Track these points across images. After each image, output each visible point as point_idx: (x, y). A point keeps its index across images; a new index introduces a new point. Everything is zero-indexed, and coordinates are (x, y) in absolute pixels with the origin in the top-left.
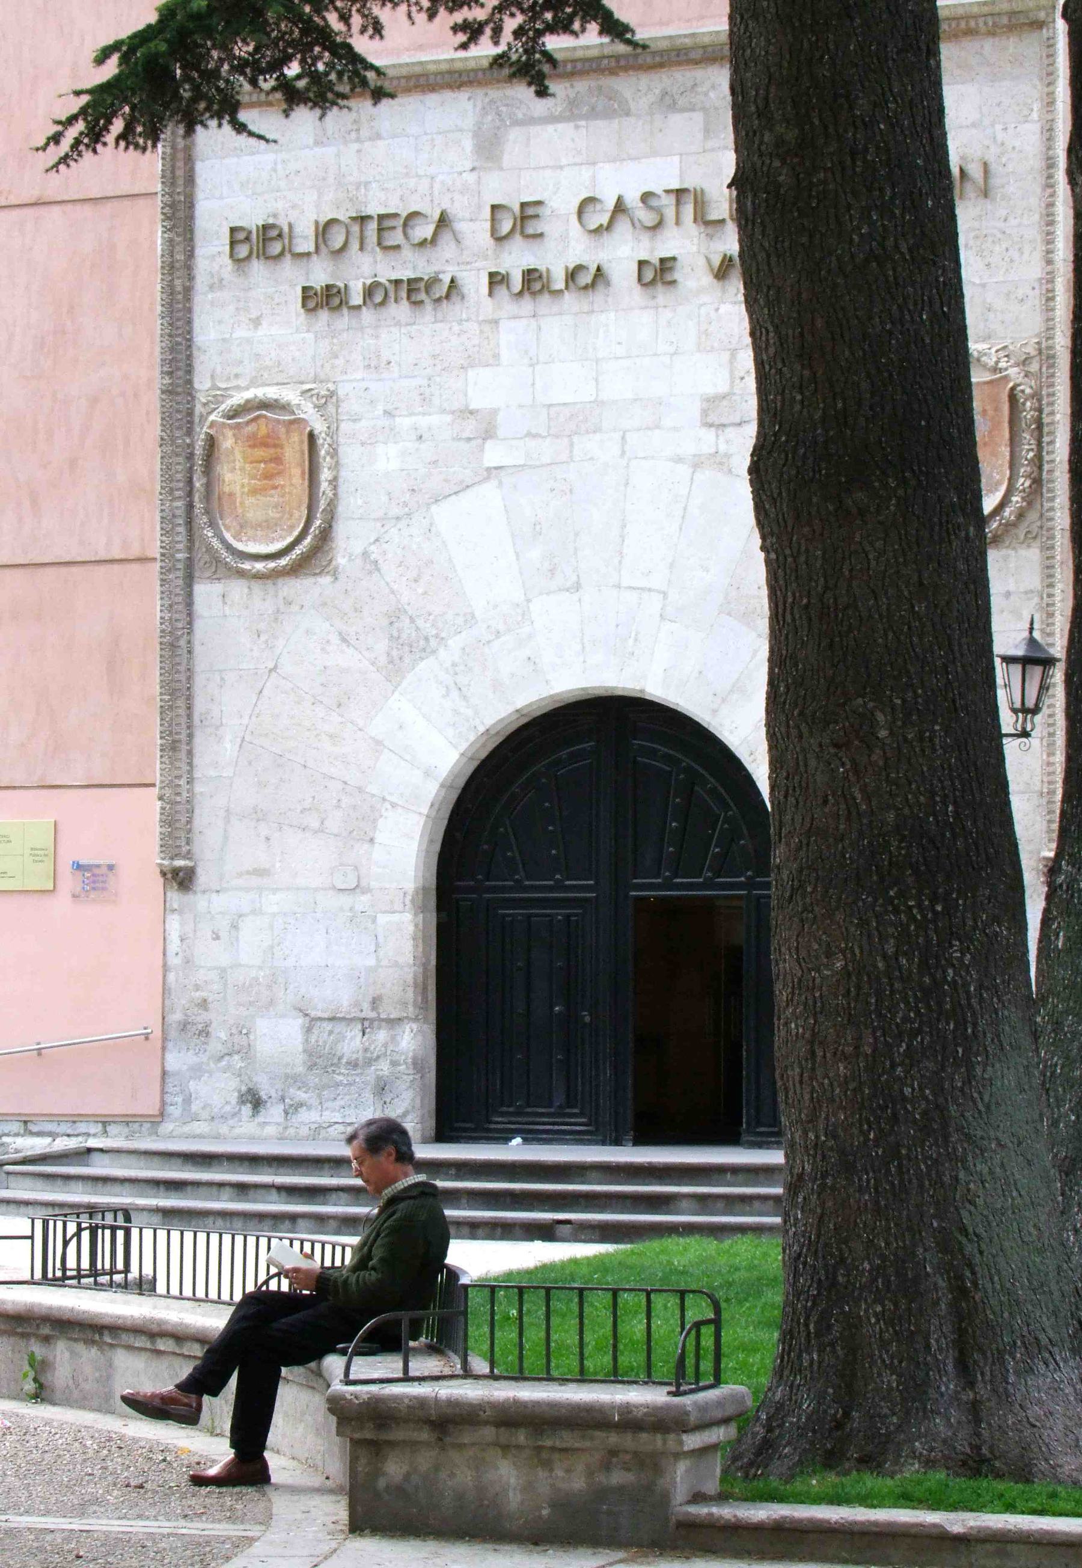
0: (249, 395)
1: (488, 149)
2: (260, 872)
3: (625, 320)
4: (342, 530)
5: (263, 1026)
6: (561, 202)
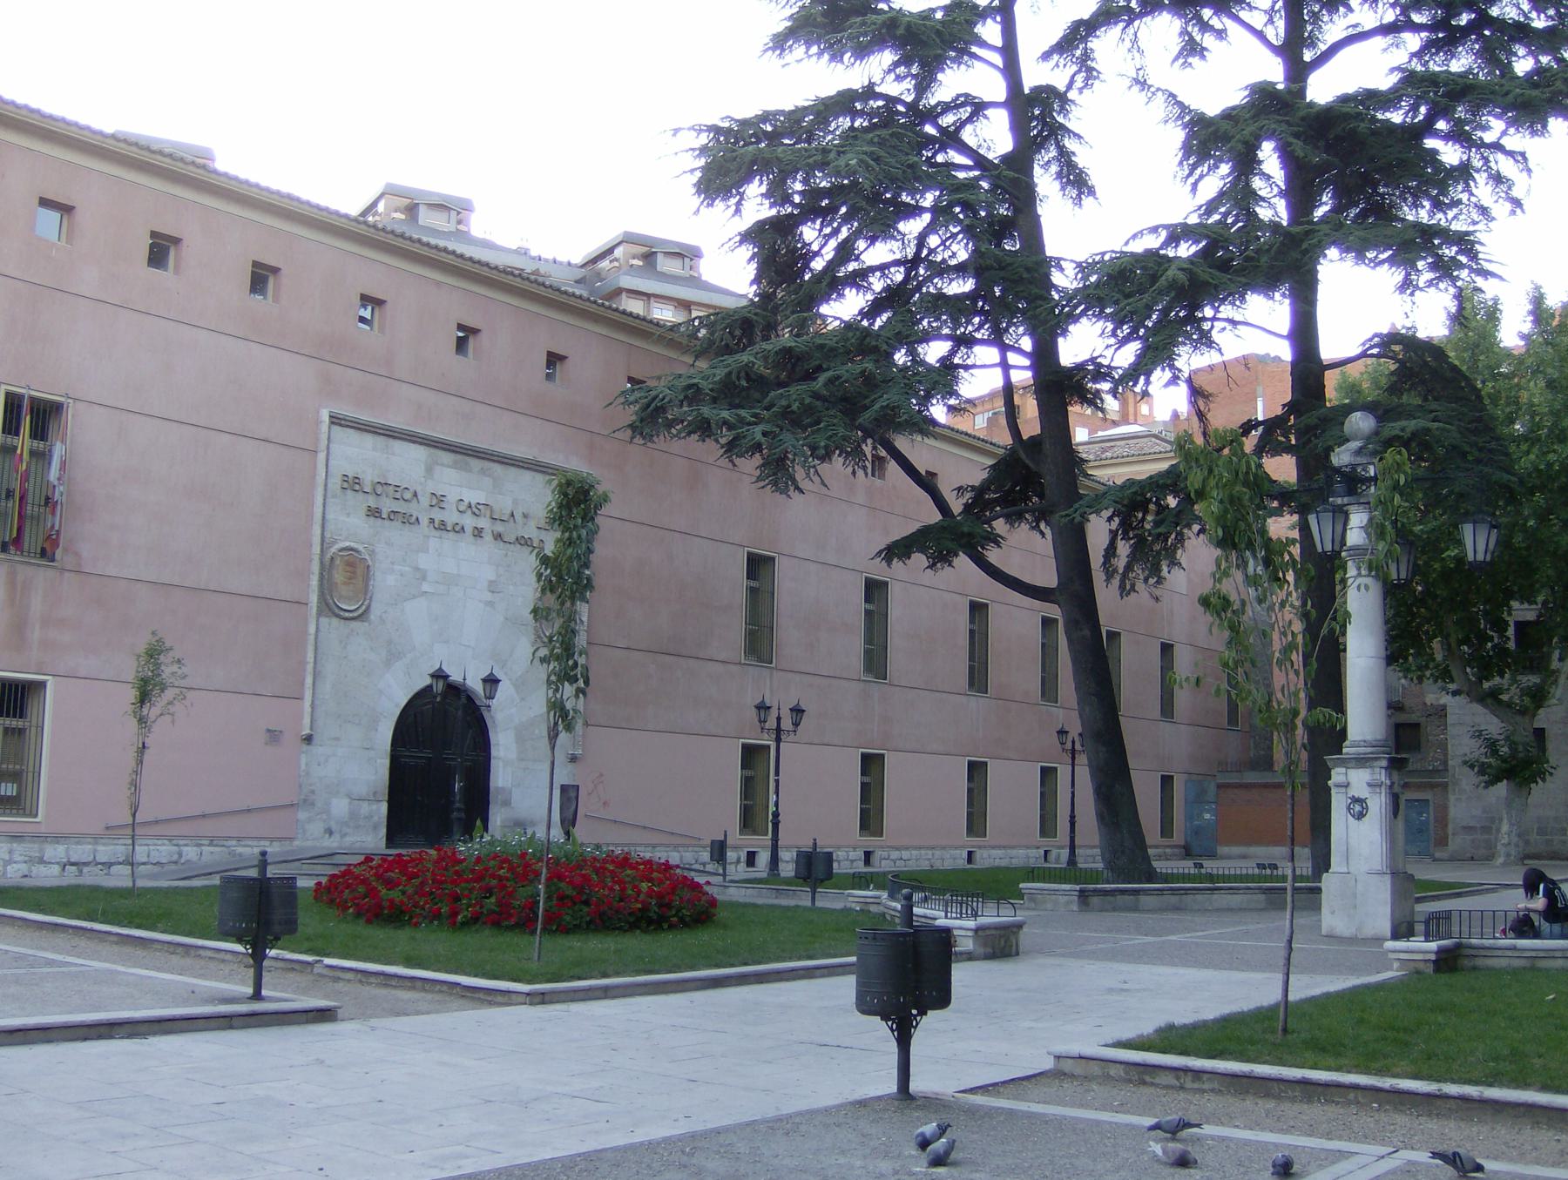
0: (347, 544)
1: (429, 470)
2: (337, 739)
3: (466, 547)
4: (374, 605)
5: (335, 801)
6: (452, 497)
